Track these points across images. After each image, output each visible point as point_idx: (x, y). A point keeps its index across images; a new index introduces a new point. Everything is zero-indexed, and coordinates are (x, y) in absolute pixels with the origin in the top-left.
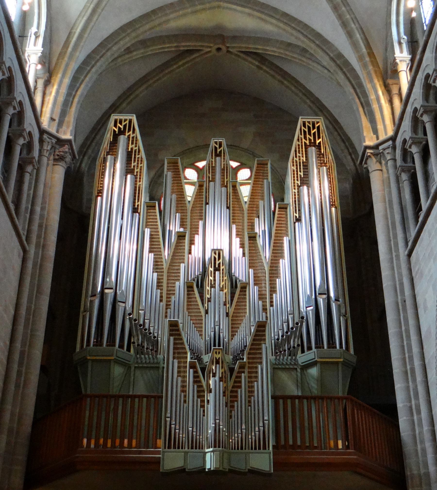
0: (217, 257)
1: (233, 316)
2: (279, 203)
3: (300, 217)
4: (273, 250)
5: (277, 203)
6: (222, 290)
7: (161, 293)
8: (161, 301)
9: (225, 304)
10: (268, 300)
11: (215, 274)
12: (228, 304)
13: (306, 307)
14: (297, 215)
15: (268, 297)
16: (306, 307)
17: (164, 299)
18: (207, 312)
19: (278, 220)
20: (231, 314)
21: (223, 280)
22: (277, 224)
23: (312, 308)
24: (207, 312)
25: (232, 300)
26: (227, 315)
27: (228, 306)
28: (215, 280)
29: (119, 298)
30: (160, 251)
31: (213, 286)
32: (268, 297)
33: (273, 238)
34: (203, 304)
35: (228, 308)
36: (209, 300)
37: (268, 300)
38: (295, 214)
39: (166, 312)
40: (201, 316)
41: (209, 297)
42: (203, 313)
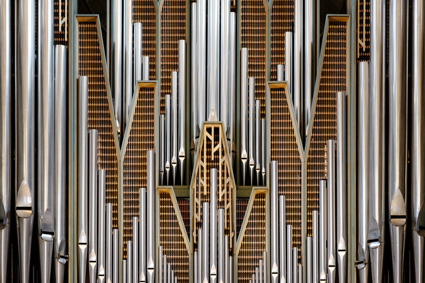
0: (212, 138)
1: (241, 253)
2: (330, 15)
3: (368, 50)
4: (319, 102)
5: (327, 15)
6: (221, 204)
7: (115, 208)
8: (115, 222)
9: (226, 232)
10: (303, 221)
11: (209, 175)
12: (233, 231)
13: (369, 241)
14: (363, 45)
15: (304, 214)
16: (369, 241)
17: (122, 221)
18: (195, 246)
19: (327, 52)
20: (237, 250)
21: (223, 188)
22: (328, 45)
23: (377, 244)
24: (195, 246)
25: (240, 222)
26: (231, 253)
27: (232, 235)
28: (209, 189)
29: (41, 226)
30: (106, 101)
31: (206, 198)
32: (304, 214)
33: (319, 77)
34: (188, 229)
35: (233, 238)
36: (200, 224)
37: (303, 221)
38: (359, 41)
39: (125, 246)
40: (186, 253)
41: (199, 220)
42: (189, 247)
